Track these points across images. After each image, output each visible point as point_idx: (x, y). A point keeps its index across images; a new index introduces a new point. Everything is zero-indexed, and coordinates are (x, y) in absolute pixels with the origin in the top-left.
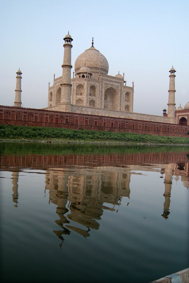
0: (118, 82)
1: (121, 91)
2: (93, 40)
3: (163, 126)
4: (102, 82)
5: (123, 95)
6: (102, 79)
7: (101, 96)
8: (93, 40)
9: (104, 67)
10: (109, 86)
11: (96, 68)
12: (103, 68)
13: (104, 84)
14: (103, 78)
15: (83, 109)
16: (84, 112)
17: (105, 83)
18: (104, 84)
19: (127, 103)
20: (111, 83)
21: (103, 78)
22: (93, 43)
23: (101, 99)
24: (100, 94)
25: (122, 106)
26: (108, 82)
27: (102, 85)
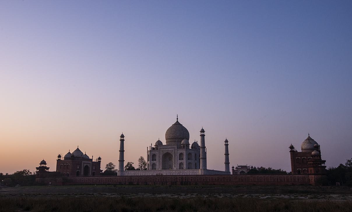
0: (172, 148)
1: (175, 153)
2: (177, 117)
4: (160, 150)
5: (177, 156)
6: (160, 148)
7: (160, 160)
8: (177, 117)
10: (165, 152)
11: (170, 138)
12: (174, 137)
14: (161, 147)
15: (129, 172)
16: (130, 174)
19: (180, 161)
21: (161, 147)
22: (177, 119)
23: (160, 161)
24: (159, 158)
25: (176, 163)
26: (164, 150)
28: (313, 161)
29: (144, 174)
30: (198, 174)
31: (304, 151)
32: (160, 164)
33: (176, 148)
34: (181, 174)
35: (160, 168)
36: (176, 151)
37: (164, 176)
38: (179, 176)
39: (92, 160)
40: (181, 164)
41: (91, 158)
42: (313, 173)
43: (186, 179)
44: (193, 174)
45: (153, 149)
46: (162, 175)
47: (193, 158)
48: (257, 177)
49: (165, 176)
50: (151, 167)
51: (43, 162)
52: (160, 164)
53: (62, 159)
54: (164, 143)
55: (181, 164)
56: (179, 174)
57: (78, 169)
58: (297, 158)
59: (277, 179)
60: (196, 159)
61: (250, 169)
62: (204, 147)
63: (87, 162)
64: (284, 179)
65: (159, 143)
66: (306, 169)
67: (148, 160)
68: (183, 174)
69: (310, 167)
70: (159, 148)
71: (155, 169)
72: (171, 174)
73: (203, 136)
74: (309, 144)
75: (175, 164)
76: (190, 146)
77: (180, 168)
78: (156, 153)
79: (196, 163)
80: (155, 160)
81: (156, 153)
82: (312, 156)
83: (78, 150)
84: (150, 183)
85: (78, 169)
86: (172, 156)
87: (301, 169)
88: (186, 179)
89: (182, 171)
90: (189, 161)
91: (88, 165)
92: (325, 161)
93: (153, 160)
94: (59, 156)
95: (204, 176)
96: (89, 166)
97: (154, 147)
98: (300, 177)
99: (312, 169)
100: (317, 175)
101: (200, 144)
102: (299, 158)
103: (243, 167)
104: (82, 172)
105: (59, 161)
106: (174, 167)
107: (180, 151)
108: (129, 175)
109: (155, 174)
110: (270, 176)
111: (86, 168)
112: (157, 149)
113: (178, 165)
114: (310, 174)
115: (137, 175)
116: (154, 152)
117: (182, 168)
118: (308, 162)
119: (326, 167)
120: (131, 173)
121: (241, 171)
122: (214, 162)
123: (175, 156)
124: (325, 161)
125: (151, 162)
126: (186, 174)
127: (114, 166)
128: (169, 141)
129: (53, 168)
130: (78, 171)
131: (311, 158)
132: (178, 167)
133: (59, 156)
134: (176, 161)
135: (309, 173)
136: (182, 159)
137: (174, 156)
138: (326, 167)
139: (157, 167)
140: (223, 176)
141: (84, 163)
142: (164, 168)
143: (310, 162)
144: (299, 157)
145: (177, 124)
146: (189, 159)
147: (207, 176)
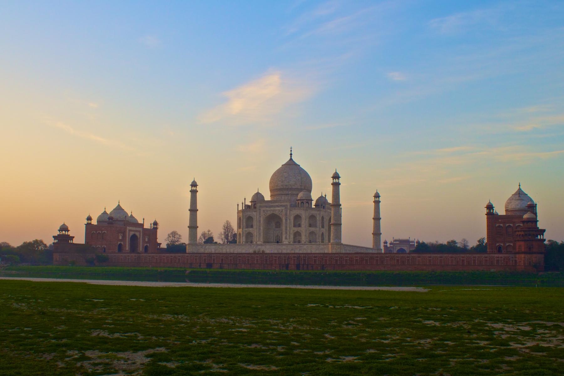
1: (286, 214)
3: (294, 257)
6: (260, 206)
9: (286, 186)
10: (269, 213)
13: (262, 212)
14: (261, 205)
17: (264, 211)
18: (262, 212)
19: (296, 229)
20: (272, 209)
21: (261, 205)
22: (291, 154)
23: (260, 229)
25: (288, 233)
26: (268, 209)
27: (260, 214)
28: (523, 231)
29: (232, 251)
30: (326, 252)
31: (509, 214)
32: (260, 234)
33: (289, 207)
34: (297, 251)
35: (259, 240)
36: (288, 211)
37: (266, 254)
38: (293, 255)
39: (142, 225)
40: (297, 235)
41: (140, 221)
42: (523, 250)
43: (305, 260)
44: (317, 252)
45: (247, 207)
46: (263, 253)
47: (319, 223)
48: (429, 257)
49: (269, 254)
50: (243, 239)
51: (64, 228)
52: (260, 234)
53: (94, 222)
54: (267, 197)
55: (297, 235)
56: (293, 252)
57: (121, 240)
58: (497, 225)
59: (463, 261)
60: (323, 227)
61: (414, 245)
62: (337, 204)
63: (134, 229)
64: (474, 261)
65: (258, 197)
66: (512, 244)
67: (239, 227)
68: (301, 252)
69: (518, 241)
70: (258, 205)
71: (252, 242)
72: (280, 252)
73: (336, 185)
74: (519, 201)
75: (286, 233)
76: (314, 203)
77: (294, 242)
78: (254, 214)
79: (323, 234)
80: (252, 226)
81: (254, 214)
82: (523, 222)
83: (119, 208)
84: (243, 266)
85: (121, 240)
86: (280, 219)
87: (502, 244)
88: (305, 260)
89: (298, 246)
90: (312, 229)
91: (137, 234)
92: (544, 231)
93: (247, 227)
94: (89, 219)
95: (337, 255)
96: (139, 236)
97: (250, 204)
98: (501, 257)
99: (522, 243)
100: (530, 253)
101: (330, 200)
102: (501, 225)
103: (402, 242)
104: (127, 246)
105: (89, 226)
106: (284, 239)
107: (296, 212)
108: (206, 252)
109: (251, 251)
110: (450, 255)
111: (134, 238)
112: (255, 208)
113: (292, 236)
114: (519, 253)
115: (221, 252)
116: (249, 213)
117: (299, 242)
118: (516, 231)
119: (544, 240)
120: (211, 249)
121: (398, 248)
122: (355, 230)
123: (286, 220)
124: (544, 231)
125: (244, 230)
126: (305, 252)
127: (180, 236)
128: (276, 193)
129: (79, 238)
130: (120, 244)
131: (522, 225)
132: (292, 240)
133: (89, 219)
134: (288, 229)
135: (517, 250)
136: (300, 226)
137: (284, 221)
138: (544, 240)
139: (255, 239)
140: (370, 255)
141: (130, 231)
142: (267, 241)
143: (520, 233)
144: (501, 223)
145: (291, 164)
146: (310, 226)
147: (342, 255)
